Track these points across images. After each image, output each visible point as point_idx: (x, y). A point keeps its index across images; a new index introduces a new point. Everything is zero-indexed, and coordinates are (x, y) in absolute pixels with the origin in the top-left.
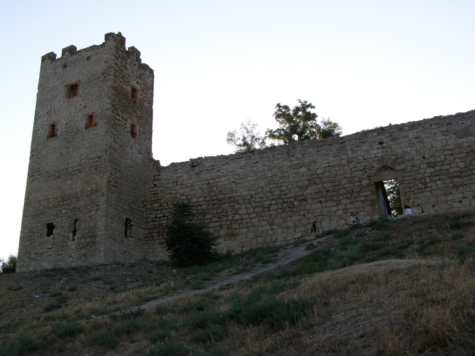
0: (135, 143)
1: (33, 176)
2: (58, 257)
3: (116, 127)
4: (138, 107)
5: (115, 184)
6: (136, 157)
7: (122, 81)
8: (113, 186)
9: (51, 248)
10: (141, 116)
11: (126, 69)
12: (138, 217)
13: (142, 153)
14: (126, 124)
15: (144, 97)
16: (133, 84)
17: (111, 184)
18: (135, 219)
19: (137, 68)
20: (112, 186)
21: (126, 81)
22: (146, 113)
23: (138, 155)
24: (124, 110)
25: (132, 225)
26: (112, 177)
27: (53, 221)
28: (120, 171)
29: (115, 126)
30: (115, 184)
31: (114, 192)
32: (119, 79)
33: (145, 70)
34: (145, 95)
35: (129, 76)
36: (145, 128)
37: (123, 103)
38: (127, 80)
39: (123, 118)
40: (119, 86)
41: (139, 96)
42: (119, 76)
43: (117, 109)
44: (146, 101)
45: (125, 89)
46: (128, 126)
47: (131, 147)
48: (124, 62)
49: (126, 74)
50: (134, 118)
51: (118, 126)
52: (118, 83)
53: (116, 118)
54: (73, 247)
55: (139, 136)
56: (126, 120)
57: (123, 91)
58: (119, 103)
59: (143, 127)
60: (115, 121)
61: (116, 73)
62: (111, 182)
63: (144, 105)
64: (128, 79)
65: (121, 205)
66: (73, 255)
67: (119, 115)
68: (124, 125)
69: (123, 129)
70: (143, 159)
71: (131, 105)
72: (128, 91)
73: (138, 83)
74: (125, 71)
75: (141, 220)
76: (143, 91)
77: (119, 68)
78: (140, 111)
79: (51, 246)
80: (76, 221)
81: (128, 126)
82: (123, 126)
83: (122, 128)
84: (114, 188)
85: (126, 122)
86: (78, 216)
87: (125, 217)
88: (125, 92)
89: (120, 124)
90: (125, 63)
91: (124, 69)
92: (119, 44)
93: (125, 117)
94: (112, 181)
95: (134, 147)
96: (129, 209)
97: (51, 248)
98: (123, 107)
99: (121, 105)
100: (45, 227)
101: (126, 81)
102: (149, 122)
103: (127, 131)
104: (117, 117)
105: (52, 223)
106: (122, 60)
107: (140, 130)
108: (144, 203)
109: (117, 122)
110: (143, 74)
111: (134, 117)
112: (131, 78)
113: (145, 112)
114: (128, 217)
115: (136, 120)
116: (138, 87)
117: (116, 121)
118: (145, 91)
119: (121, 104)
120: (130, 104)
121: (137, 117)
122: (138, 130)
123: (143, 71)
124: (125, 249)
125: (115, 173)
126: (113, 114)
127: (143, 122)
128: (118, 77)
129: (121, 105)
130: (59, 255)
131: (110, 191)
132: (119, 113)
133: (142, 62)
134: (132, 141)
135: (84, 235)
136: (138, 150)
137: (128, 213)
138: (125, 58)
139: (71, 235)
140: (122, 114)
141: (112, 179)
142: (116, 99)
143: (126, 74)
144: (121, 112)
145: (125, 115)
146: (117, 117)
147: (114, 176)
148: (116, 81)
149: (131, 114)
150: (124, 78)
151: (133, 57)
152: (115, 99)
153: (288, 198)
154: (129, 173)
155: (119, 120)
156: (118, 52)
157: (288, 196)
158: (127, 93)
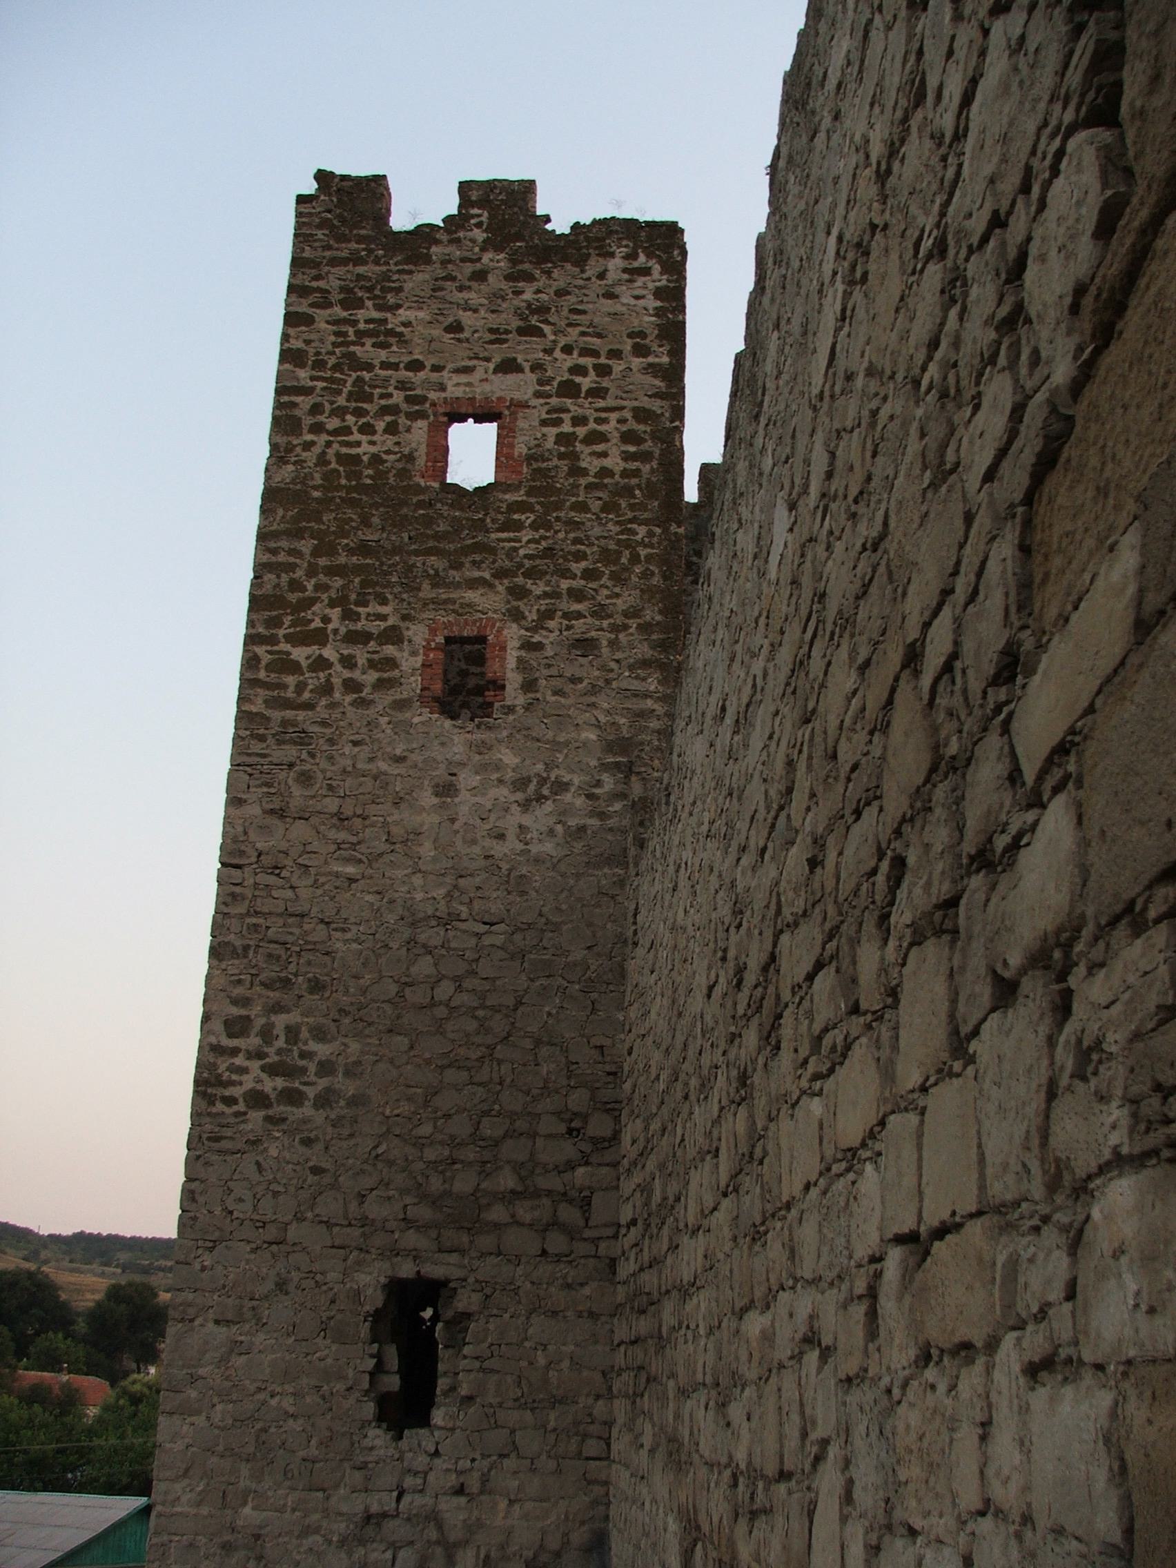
0: (482, 748)
3: (285, 723)
4: (522, 507)
5: (272, 1085)
6: (501, 837)
7: (350, 419)
8: (257, 1099)
10: (549, 552)
11: (383, 335)
13: (561, 787)
14: (391, 663)
15: (579, 421)
16: (459, 392)
17: (236, 1091)
19: (504, 285)
20: (241, 1107)
21: (394, 410)
22: (606, 508)
23: (516, 817)
24: (364, 584)
25: (467, 1316)
26: (253, 1041)
28: (316, 986)
29: (277, 715)
30: (272, 1085)
31: (255, 1143)
32: (317, 428)
33: (581, 263)
34: (585, 407)
35: (416, 366)
36: (600, 612)
37: (363, 549)
38: (398, 397)
39: (355, 638)
40: (322, 460)
42: (316, 409)
43: (312, 601)
44: (596, 437)
45: (376, 459)
46: (409, 662)
47: (446, 790)
48: (369, 312)
49: (395, 367)
50: (471, 596)
51: (309, 706)
52: (310, 457)
55: (529, 686)
57: (358, 475)
58: (323, 561)
59: (566, 616)
60: (284, 687)
61: (294, 405)
62: (232, 1083)
64: (402, 386)
65: (329, 1206)
67: (319, 637)
68: (372, 676)
69: (362, 703)
70: (573, 822)
71: (442, 527)
72: (410, 458)
73: (508, 366)
75: (558, 1258)
76: (569, 389)
77: (319, 364)
78: (534, 526)
81: (409, 662)
82: (351, 686)
83: (349, 699)
84: (257, 1116)
85: (390, 650)
87: (370, 1281)
88: (380, 475)
89: (327, 689)
90: (379, 308)
91: (366, 351)
92: (320, 234)
93: (376, 627)
94: (243, 1071)
95: (467, 779)
96: (424, 1213)
98: (358, 570)
101: (385, 410)
102: (635, 559)
103: (401, 705)
104: (300, 654)
107: (539, 647)
108: (599, 1126)
109: (301, 687)
110: (560, 293)
111: (473, 584)
112: (437, 368)
113: (596, 506)
114: (406, 1270)
115: (489, 602)
116: (521, 386)
117: (291, 680)
118: (586, 383)
119: (342, 559)
120: (429, 521)
121: (500, 574)
123: (562, 276)
124: (380, 1501)
125: (278, 1008)
126: (260, 650)
127: (565, 584)
128: (308, 421)
129: (331, 571)
131: (225, 1144)
132: (317, 623)
133: (560, 225)
134: (454, 740)
136: (521, 783)
137: (412, 1239)
138: (386, 277)
140: (348, 615)
141: (239, 1061)
142: (291, 552)
143: (395, 367)
144: (335, 613)
146: (300, 654)
147: (267, 1034)
148: (290, 449)
149: (437, 581)
150: (369, 398)
151: (458, 240)
152: (282, 557)
155: (321, 664)
156: (317, 278)
158: (403, 474)
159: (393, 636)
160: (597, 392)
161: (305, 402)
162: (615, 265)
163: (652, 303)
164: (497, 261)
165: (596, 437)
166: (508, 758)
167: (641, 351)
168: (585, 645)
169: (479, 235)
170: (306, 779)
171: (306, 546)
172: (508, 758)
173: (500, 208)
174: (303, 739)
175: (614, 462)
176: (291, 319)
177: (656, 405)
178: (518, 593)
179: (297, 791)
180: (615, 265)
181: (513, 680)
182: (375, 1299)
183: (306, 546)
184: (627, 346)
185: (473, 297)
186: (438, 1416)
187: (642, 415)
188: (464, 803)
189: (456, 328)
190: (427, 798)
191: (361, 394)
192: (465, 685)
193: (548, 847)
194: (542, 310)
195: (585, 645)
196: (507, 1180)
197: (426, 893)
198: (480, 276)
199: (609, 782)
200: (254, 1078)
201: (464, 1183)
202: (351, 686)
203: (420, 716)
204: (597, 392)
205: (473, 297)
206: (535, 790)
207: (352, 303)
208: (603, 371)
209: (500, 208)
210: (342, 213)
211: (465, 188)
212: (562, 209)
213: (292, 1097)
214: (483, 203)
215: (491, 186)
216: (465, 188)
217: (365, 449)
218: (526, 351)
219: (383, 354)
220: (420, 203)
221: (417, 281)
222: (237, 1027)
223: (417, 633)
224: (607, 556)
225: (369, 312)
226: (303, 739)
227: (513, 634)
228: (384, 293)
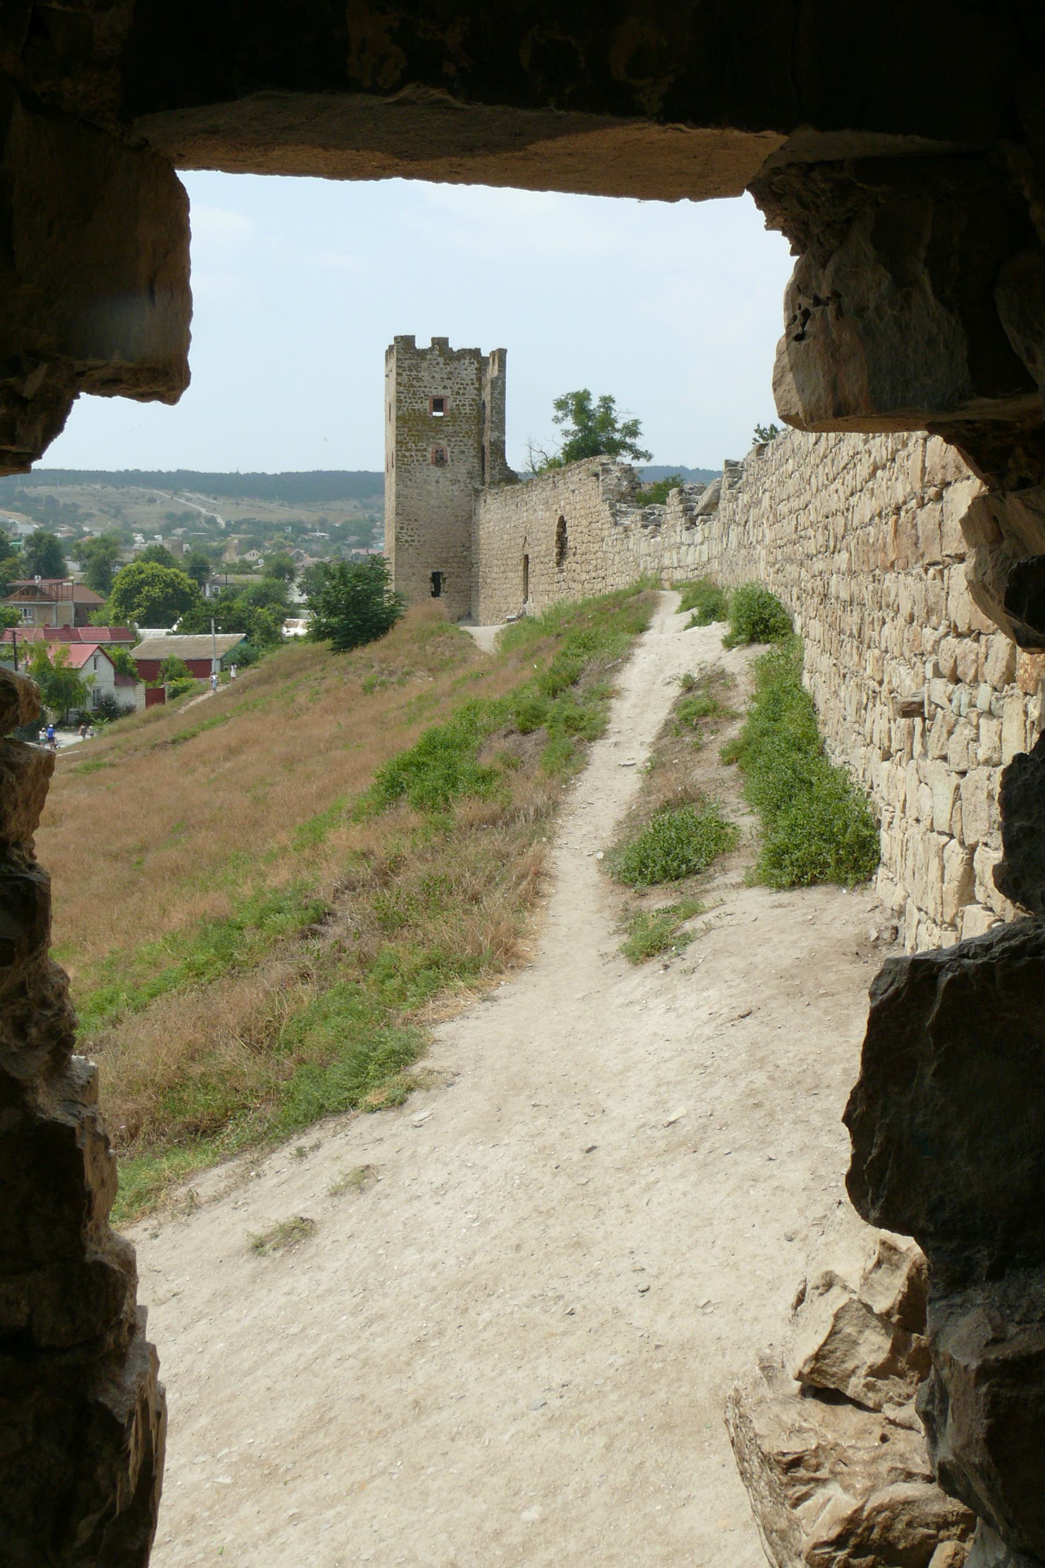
5: (409, 539)
8: (406, 541)
11: (418, 379)
12: (454, 565)
16: (434, 394)
18: (449, 570)
30: (409, 539)
33: (459, 361)
37: (417, 431)
39: (419, 450)
41: (449, 404)
44: (464, 405)
46: (429, 456)
47: (437, 482)
48: (414, 373)
53: (404, 456)
56: (425, 450)
63: (460, 413)
67: (410, 450)
73: (445, 387)
74: (418, 384)
76: (458, 393)
81: (429, 456)
82: (418, 461)
87: (429, 573)
91: (414, 383)
99: (413, 435)
104: (407, 454)
106: (411, 370)
108: (467, 545)
114: (435, 571)
115: (444, 443)
116: (447, 392)
118: (461, 392)
122: (449, 454)
123: (456, 364)
129: (413, 435)
133: (455, 349)
134: (436, 472)
145: (423, 445)
146: (407, 454)
149: (433, 438)
154: (435, 516)
155: (411, 456)
159: (425, 450)
160: (464, 394)
161: (403, 396)
162: (467, 361)
163: (475, 371)
164: (441, 360)
165: (464, 405)
166: (449, 475)
167: (473, 384)
168: (463, 452)
169: (437, 353)
170: (410, 480)
171: (406, 430)
172: (449, 475)
173: (440, 343)
174: (409, 472)
175: (468, 411)
176: (398, 374)
177: (476, 398)
178: (449, 440)
179: (409, 483)
180: (467, 361)
181: (449, 459)
182: (430, 576)
183: (406, 430)
184: (469, 382)
185: (437, 369)
186: (442, 595)
187: (473, 400)
188: (440, 485)
189: (433, 377)
190: (434, 483)
191: (414, 394)
192: (440, 460)
193: (456, 493)
194: (451, 373)
195: (463, 452)
196: (452, 554)
197: (433, 502)
198: (438, 364)
199: (468, 481)
200: (406, 538)
201: (444, 555)
202: (418, 461)
203: (432, 467)
204: (464, 394)
205: (437, 369)
206: (455, 482)
207: (411, 370)
208: (465, 389)
209: (440, 343)
210: (404, 345)
211: (433, 339)
212: (455, 345)
213: (413, 541)
214: (438, 344)
215: (439, 339)
216: (433, 339)
217: (416, 407)
218: (449, 383)
219: (418, 384)
220: (423, 343)
221: (425, 364)
222: (402, 528)
223: (430, 449)
224: (467, 433)
225: (414, 373)
226: (409, 472)
227: (449, 449)
228: (417, 367)
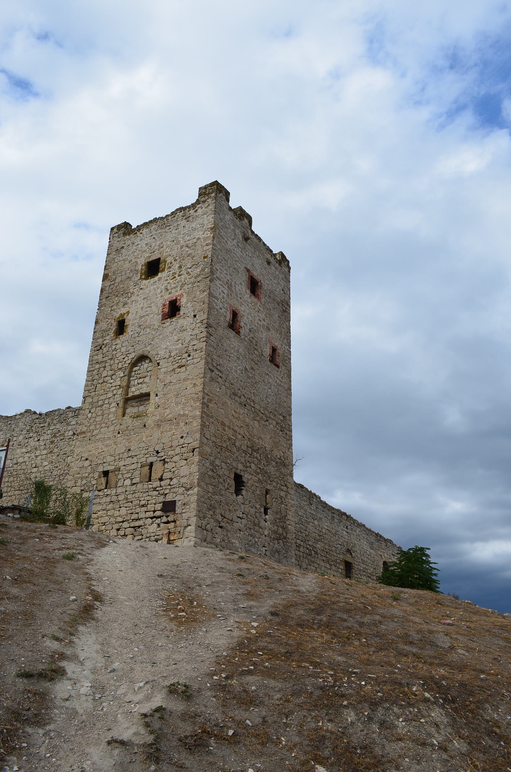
1: (213, 371)
2: (250, 538)
9: (240, 518)
27: (242, 474)
54: (266, 533)
66: (266, 544)
79: (241, 516)
80: (267, 492)
86: (269, 487)
97: (240, 518)
100: (232, 476)
105: (241, 476)
130: (252, 535)
135: (276, 521)
139: (262, 510)
153: (310, 545)
157: (310, 543)
